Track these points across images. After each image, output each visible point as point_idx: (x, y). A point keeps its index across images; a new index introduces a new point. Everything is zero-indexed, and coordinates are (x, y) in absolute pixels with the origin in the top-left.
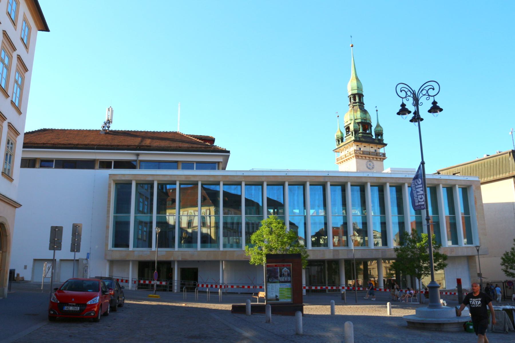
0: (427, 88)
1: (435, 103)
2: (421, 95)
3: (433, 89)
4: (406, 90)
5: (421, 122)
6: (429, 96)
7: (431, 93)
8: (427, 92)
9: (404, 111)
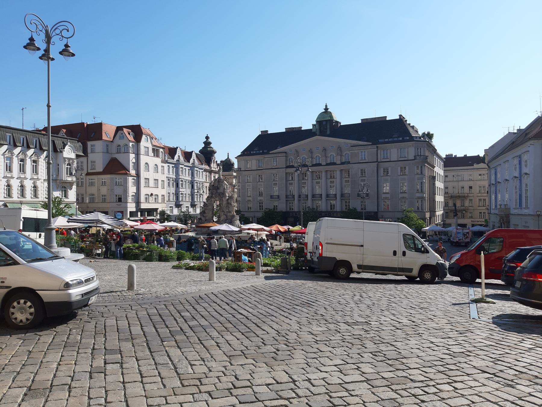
0: (61, 28)
1: (67, 46)
2: (54, 34)
3: (68, 31)
4: (37, 23)
5: (50, 62)
6: (62, 36)
7: (65, 33)
8: (61, 32)
9: (31, 45)
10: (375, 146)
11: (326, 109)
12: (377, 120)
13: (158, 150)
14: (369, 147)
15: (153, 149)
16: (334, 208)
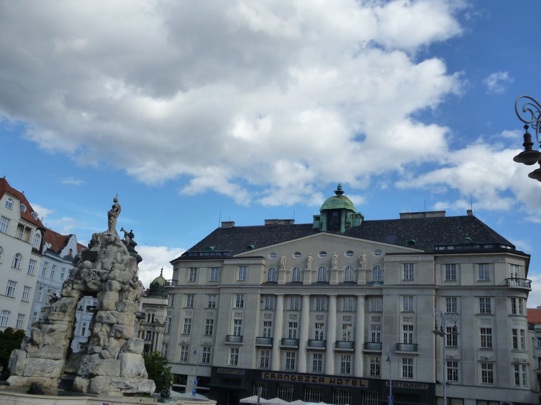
10: (431, 258)
11: (339, 192)
12: (428, 216)
13: (29, 230)
14: (420, 258)
15: (20, 226)
16: (348, 371)
